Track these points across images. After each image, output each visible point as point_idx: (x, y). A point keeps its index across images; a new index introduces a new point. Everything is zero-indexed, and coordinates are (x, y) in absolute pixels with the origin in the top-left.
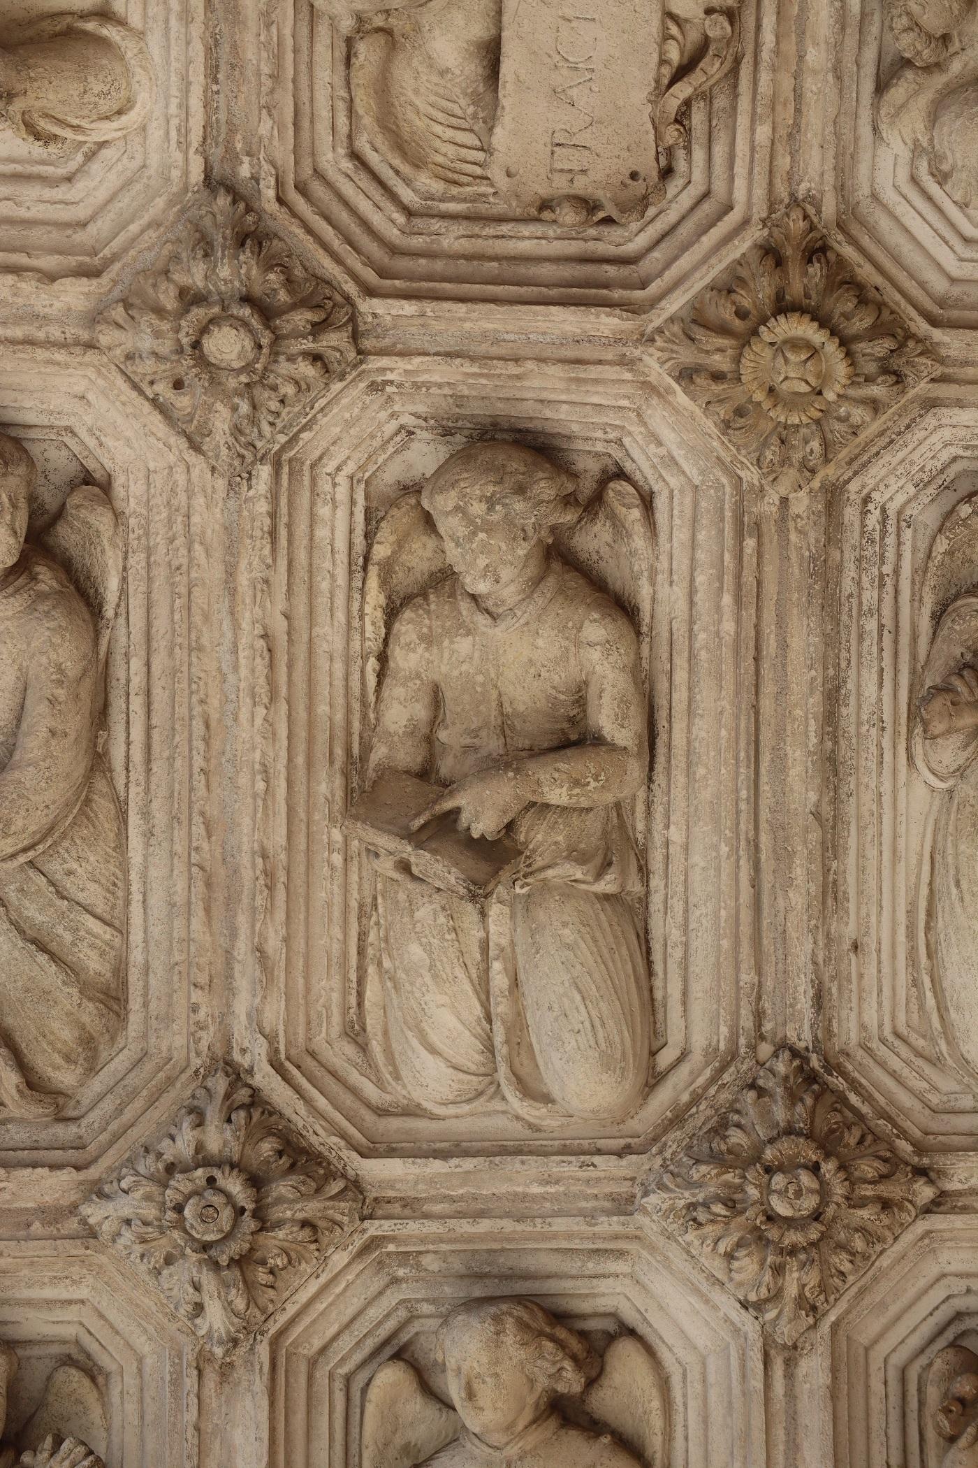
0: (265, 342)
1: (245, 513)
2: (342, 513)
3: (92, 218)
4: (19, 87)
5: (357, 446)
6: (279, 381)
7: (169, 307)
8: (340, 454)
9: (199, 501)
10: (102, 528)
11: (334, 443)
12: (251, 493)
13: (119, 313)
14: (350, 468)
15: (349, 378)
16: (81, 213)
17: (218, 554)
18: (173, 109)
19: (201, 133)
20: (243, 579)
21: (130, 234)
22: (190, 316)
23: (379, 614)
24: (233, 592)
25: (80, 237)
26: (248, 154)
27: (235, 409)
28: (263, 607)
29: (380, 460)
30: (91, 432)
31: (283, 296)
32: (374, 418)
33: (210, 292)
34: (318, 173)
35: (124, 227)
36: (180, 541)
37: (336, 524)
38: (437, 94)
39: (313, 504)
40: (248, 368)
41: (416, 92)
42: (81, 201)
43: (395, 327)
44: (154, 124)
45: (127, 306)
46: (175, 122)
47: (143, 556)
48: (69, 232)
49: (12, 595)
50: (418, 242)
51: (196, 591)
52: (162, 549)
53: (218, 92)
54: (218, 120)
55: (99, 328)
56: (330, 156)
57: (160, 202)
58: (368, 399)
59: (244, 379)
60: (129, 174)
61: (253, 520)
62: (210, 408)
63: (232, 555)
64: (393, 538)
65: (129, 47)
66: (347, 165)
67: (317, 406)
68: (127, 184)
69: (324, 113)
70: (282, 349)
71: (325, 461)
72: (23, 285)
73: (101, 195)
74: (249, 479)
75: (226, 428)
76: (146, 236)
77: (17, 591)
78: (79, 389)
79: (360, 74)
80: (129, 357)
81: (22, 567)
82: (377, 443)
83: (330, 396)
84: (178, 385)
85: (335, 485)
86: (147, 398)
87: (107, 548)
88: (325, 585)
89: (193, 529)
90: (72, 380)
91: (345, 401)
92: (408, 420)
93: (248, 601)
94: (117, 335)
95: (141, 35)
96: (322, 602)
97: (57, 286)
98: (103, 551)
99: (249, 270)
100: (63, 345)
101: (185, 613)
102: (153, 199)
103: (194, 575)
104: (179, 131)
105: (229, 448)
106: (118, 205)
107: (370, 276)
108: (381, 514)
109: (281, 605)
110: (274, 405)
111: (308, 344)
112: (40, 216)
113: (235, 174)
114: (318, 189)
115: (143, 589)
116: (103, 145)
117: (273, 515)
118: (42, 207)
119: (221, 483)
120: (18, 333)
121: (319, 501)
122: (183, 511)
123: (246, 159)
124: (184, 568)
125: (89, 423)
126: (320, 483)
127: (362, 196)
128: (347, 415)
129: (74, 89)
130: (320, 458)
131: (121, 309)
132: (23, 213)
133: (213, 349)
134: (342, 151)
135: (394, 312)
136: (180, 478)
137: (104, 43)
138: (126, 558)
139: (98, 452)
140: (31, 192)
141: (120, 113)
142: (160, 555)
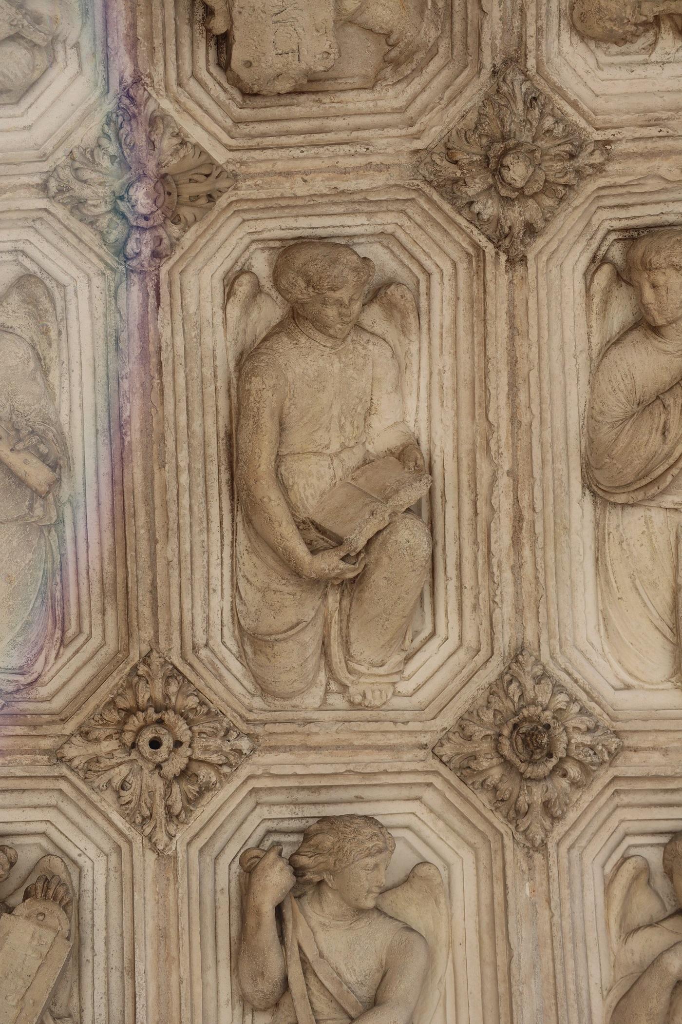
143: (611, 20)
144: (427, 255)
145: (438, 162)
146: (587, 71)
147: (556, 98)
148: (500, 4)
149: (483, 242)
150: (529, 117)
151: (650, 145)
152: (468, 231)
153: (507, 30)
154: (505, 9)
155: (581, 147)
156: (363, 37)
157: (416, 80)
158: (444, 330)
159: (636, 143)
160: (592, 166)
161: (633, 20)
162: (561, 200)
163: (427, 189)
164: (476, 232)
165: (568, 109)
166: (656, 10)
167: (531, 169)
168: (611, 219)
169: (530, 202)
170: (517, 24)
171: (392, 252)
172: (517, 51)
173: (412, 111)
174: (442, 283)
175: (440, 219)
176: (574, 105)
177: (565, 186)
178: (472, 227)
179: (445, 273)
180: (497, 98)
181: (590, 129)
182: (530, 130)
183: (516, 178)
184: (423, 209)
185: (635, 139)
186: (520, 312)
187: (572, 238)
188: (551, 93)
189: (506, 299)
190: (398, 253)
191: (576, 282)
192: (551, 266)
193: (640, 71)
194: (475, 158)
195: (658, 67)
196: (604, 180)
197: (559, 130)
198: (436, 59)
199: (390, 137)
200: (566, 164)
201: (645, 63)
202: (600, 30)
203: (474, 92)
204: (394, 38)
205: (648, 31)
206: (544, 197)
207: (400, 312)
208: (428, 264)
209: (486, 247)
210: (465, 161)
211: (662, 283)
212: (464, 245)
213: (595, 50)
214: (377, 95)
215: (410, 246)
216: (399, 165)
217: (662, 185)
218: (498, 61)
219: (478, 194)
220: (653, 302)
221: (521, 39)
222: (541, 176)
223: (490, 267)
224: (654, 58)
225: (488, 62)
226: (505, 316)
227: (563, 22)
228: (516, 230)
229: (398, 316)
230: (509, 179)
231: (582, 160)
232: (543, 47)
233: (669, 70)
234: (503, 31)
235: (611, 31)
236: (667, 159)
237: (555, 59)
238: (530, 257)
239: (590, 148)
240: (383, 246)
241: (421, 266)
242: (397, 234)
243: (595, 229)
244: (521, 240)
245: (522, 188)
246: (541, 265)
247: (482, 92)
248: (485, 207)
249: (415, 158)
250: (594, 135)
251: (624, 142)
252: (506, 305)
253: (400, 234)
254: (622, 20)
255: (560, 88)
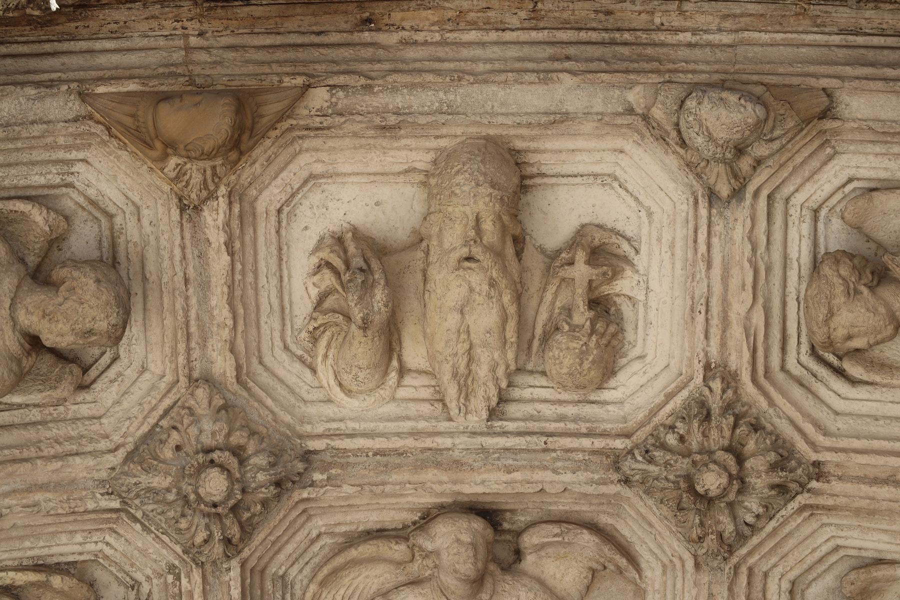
0: (219, 510)
1: (84, 493)
2: (77, 548)
3: (267, 369)
4: (369, 333)
5: (125, 556)
6: (190, 518)
7: (231, 439)
8: (119, 545)
9: (90, 462)
10: (59, 391)
11: (127, 540)
12: (99, 496)
13: (218, 402)
14: (108, 551)
15: (185, 557)
16: (267, 359)
17: (55, 477)
18: (352, 425)
19: (341, 447)
20: (38, 497)
21: (265, 399)
22: (232, 458)
23: (8, 582)
24: (29, 490)
25: (255, 361)
26: (328, 478)
27: (168, 490)
28: (21, 512)
29: (112, 569)
30: (120, 374)
31: (246, 515)
32: (146, 566)
33: (246, 467)
34: (309, 518)
35: (269, 395)
36: (59, 449)
37: (66, 547)
38: (364, 588)
39: (83, 531)
40: (199, 499)
41: (367, 577)
42: (275, 358)
43: (221, 583)
44: (336, 410)
45: (225, 407)
46: (342, 425)
47: (39, 418)
48: (256, 353)
49: (20, 343)
50: (269, 585)
51: (28, 466)
52: (48, 434)
53: (367, 456)
54: (348, 456)
55: (206, 387)
56: (321, 523)
57: (288, 418)
58: (163, 564)
59: (192, 497)
60: (297, 390)
61: (81, 499)
62: (167, 474)
63: (55, 487)
64: (66, 588)
65: (385, 392)
66: (314, 533)
67: (164, 537)
68: (292, 391)
69: (349, 518)
70: (213, 520)
71: (114, 535)
72: (227, 330)
73: (281, 372)
74: (108, 493)
75: (155, 484)
76: (267, 412)
77: (22, 345)
78: (152, 366)
79: (386, 548)
80: (191, 411)
81: (34, 343)
82: (127, 568)
83: (171, 545)
84: (178, 448)
85: (96, 542)
86: (159, 420)
87: (44, 394)
88: (27, 544)
89: (70, 458)
90: (159, 363)
91: (164, 552)
92: (145, 588)
93: (24, 501)
94: (205, 403)
95: (393, 399)
96: (17, 544)
97: (228, 354)
98: (40, 391)
99: (264, 493)
100: (189, 360)
101: (10, 458)
102: (289, 413)
103: (39, 462)
104: (338, 429)
105: (136, 484)
106: (278, 386)
107: (251, 564)
108: (72, 571)
109: (19, 522)
110: (171, 514)
111: (218, 535)
112: (262, 331)
113: (314, 470)
114: (304, 518)
115: (17, 421)
116: (314, 371)
117: (86, 512)
118: (268, 332)
119: (104, 475)
120: (193, 329)
121: (85, 534)
122: (81, 450)
123: (325, 477)
124: (41, 454)
125: (125, 373)
126: (98, 533)
127: (295, 545)
128: (151, 551)
129: (363, 362)
130: (115, 532)
131: (222, 402)
132: (263, 319)
133: (211, 475)
134: (323, 529)
135: (232, 583)
136: (103, 445)
137: (386, 373)
138: (36, 406)
139: (104, 379)
140: (277, 325)
141: (340, 385)
142: (44, 433)
143: (581, 365)
144: (814, 550)
145: (704, 551)
146: (645, 373)
147: (656, 420)
148: (559, 473)
149: (794, 505)
150: (662, 462)
151: (715, 322)
152: (781, 520)
153: (585, 465)
154: (564, 468)
155: (703, 404)
156: (596, 592)
157: (637, 549)
158: (893, 541)
159: (712, 336)
160: (724, 391)
161: (585, 339)
162: (756, 427)
163: (734, 560)
164: (783, 512)
165: (668, 408)
166: (582, 310)
167: (712, 466)
168: (798, 354)
169: (748, 464)
170: (580, 456)
171: (814, 580)
172: (608, 457)
173: (665, 560)
174: (847, 538)
175: (771, 544)
176: (669, 397)
177: (735, 426)
178: (778, 516)
179: (834, 534)
180: (647, 486)
181: (692, 385)
182: (676, 462)
183: (718, 483)
184: (760, 559)
185: (707, 337)
186: (872, 473)
187: (808, 403)
188: (652, 425)
189: (856, 486)
190: (815, 575)
191: (859, 397)
192: (833, 428)
193: (652, 315)
194: (697, 521)
195: (650, 294)
196: (743, 375)
197: (681, 427)
198: (618, 527)
199: (683, 589)
200: (713, 424)
201: (646, 305)
202: (592, 373)
203: (642, 504)
204: (595, 566)
205: (615, 302)
206: (746, 448)
207: (871, 583)
208: (825, 549)
209: (800, 503)
210: (699, 532)
211: (845, 332)
212: (799, 520)
213: (629, 358)
214: (649, 588)
215: (805, 566)
216: (710, 583)
217: (759, 308)
218: (615, 477)
219: (734, 518)
220: (865, 340)
221: (594, 452)
222: (720, 455)
223: (821, 501)
224: (641, 297)
225: (612, 489)
226: (874, 489)
227: (593, 397)
228: (777, 480)
229: (875, 586)
230: (718, 491)
231: (715, 404)
232: (608, 426)
233: (653, 285)
234: (586, 470)
235: (593, 362)
236: (731, 304)
237: (626, 409)
238: (814, 457)
239: (706, 392)
240: (807, 588)
241: (828, 554)
242: (792, 578)
243: (806, 372)
244: (791, 472)
245: (730, 476)
246: (827, 442)
247: (644, 496)
248: (749, 510)
249: (705, 567)
250: (697, 382)
251: (709, 349)
252: (862, 486)
253: (791, 576)
254: (582, 352)
255: (651, 411)
